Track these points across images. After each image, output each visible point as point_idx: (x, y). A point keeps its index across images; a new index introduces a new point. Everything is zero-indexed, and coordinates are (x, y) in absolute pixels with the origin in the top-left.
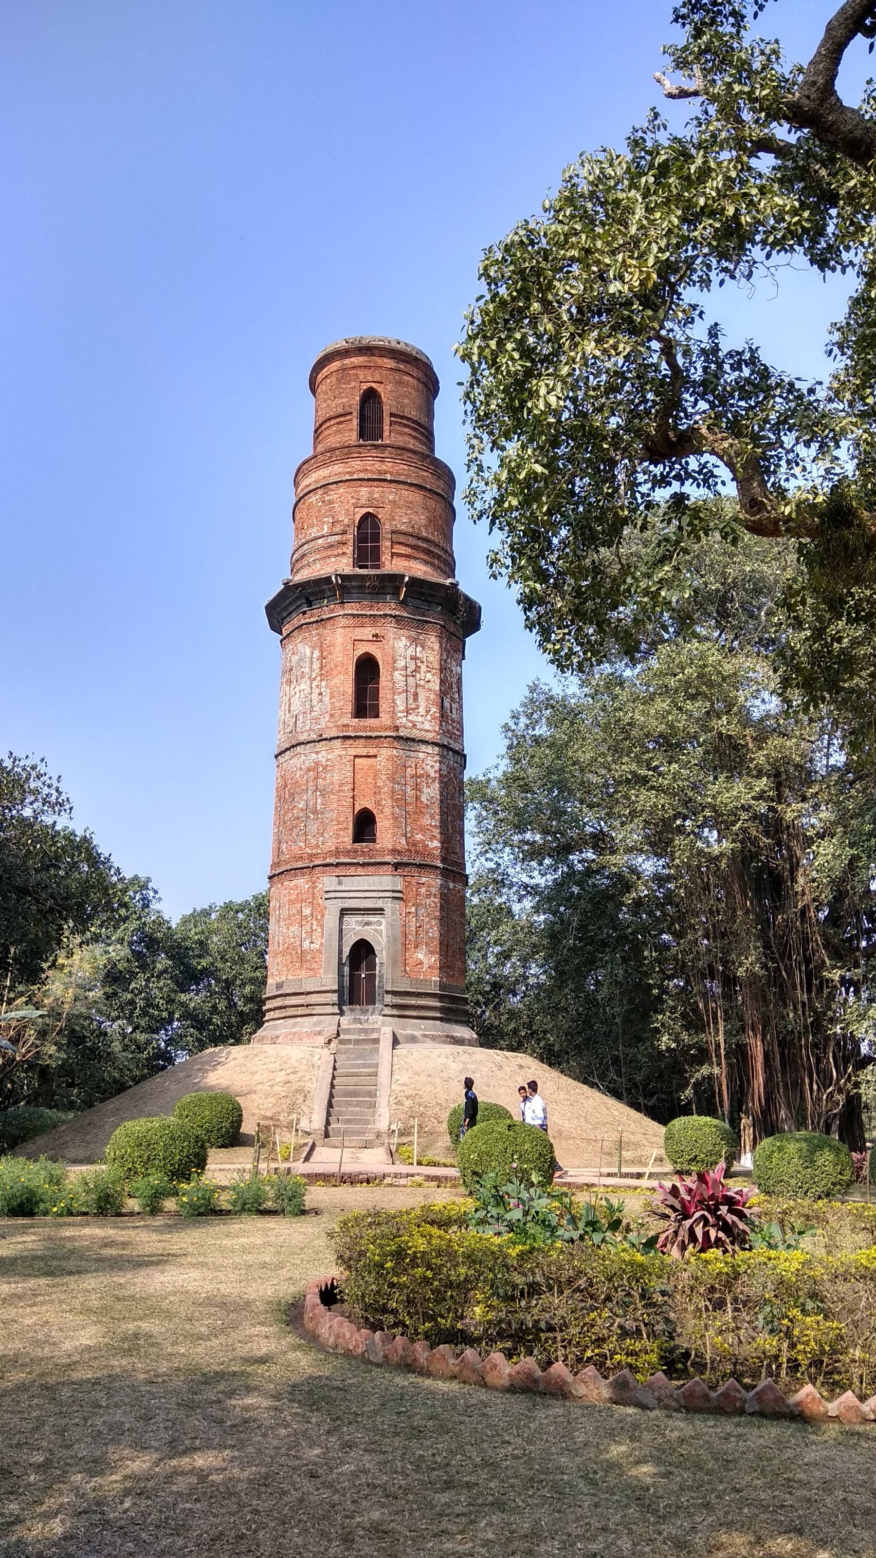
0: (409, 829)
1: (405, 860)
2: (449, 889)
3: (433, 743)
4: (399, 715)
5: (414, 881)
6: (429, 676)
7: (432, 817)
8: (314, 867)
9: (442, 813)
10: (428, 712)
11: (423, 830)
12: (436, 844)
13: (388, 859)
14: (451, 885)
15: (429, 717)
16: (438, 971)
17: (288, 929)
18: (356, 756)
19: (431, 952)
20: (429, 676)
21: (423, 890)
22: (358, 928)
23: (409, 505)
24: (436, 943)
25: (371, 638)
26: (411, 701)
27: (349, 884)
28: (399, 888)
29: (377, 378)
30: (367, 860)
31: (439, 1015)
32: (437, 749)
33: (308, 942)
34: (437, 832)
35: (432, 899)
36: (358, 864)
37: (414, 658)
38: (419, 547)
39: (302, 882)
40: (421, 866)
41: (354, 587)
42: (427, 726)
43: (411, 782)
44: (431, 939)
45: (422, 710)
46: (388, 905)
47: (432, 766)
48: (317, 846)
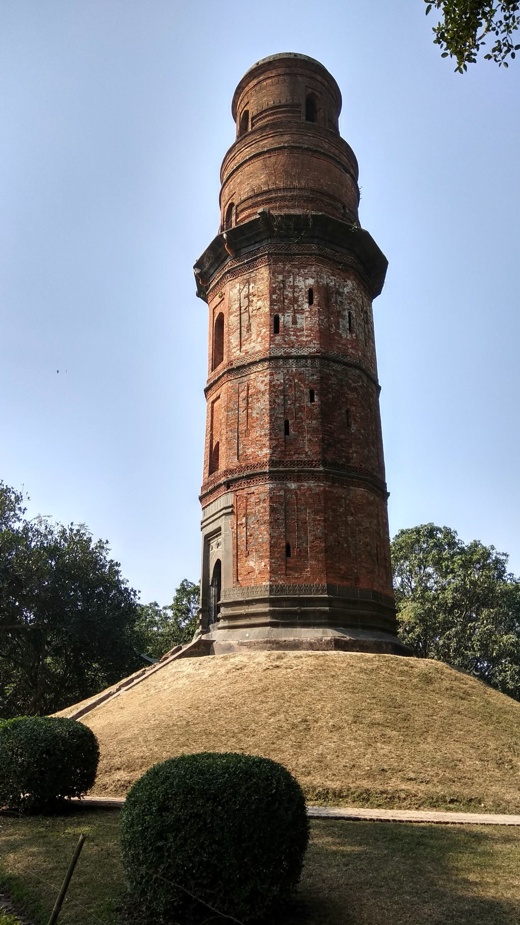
0: (241, 446)
1: (236, 476)
2: (288, 490)
3: (262, 361)
4: (233, 351)
5: (244, 493)
6: (260, 303)
7: (262, 427)
9: (271, 422)
10: (258, 335)
11: (254, 442)
12: (266, 451)
14: (293, 486)
15: (260, 339)
16: (267, 576)
18: (213, 402)
19: (261, 558)
20: (260, 303)
21: (253, 499)
23: (251, 176)
24: (267, 547)
25: (220, 300)
26: (244, 333)
29: (246, 101)
31: (268, 620)
32: (266, 364)
34: (266, 441)
37: (247, 296)
38: (257, 203)
40: (248, 477)
41: (209, 269)
42: (258, 348)
43: (243, 404)
45: (254, 337)
46: (222, 523)
47: (262, 382)
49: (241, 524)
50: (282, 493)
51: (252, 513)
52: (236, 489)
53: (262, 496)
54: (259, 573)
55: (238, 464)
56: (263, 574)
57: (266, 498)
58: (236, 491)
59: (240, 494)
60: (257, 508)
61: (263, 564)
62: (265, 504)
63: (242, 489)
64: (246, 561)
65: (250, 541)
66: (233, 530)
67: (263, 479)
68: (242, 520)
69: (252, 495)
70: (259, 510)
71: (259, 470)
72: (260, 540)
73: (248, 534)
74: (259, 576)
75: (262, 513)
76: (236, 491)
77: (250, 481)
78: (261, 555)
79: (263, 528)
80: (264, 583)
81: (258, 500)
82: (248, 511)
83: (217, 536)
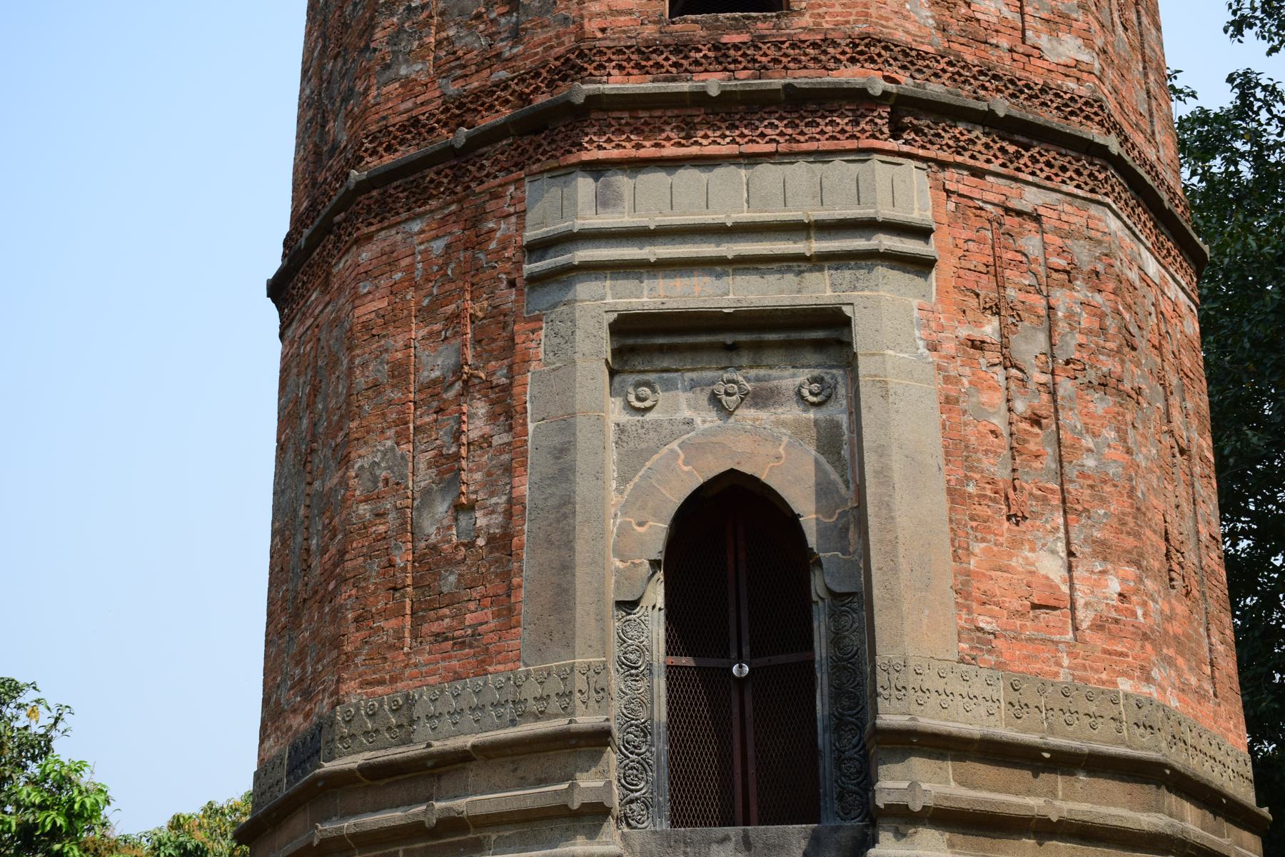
1: (936, 89)
2: (1144, 277)
8: (475, 143)
13: (849, 75)
14: (1152, 268)
17: (345, 461)
19: (1103, 550)
21: (1031, 243)
22: (706, 419)
27: (648, 200)
28: (918, 214)
30: (744, 80)
33: (442, 508)
35: (1081, 291)
36: (700, 98)
39: (419, 237)
44: (1097, 483)
48: (492, 59)
49: (978, 345)
50: (1133, 275)
51: (1031, 310)
52: (945, 156)
53: (1083, 254)
54: (1098, 626)
55: (939, 41)
56: (1112, 636)
57: (1100, 267)
58: (943, 165)
59: (963, 189)
60: (1061, 298)
61: (1114, 586)
62: (1098, 299)
63: (978, 173)
64: (1016, 543)
65: (1032, 446)
66: (932, 357)
67: (1078, 172)
68: (978, 324)
69: (1030, 225)
70: (1070, 315)
71: (1050, 117)
72: (1090, 462)
73: (1020, 406)
74: (1098, 641)
75: (1090, 332)
76: (943, 165)
77: (1018, 156)
78: (1097, 534)
79: (1100, 404)
80: (1125, 685)
81: (1062, 263)
82: (1011, 292)
83: (733, 348)
